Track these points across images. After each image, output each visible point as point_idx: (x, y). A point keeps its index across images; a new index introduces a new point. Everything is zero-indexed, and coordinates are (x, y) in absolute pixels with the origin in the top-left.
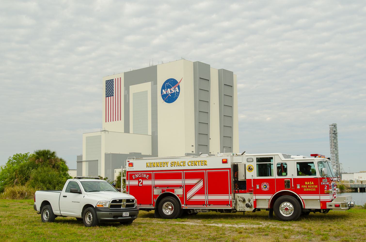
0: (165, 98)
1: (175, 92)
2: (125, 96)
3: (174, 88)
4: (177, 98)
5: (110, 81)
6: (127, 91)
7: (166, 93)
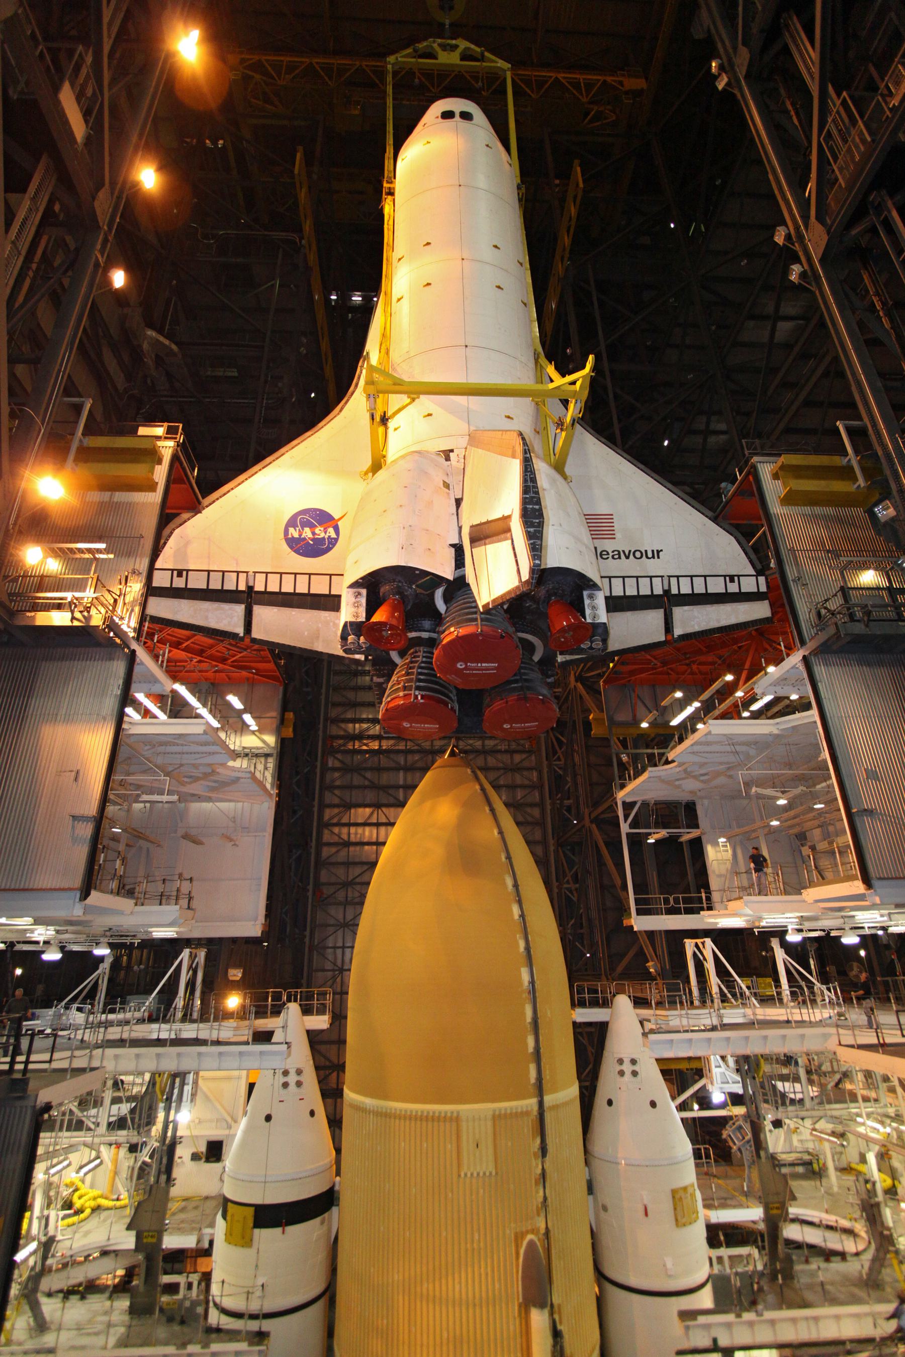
4: (329, 549)
7: (300, 535)
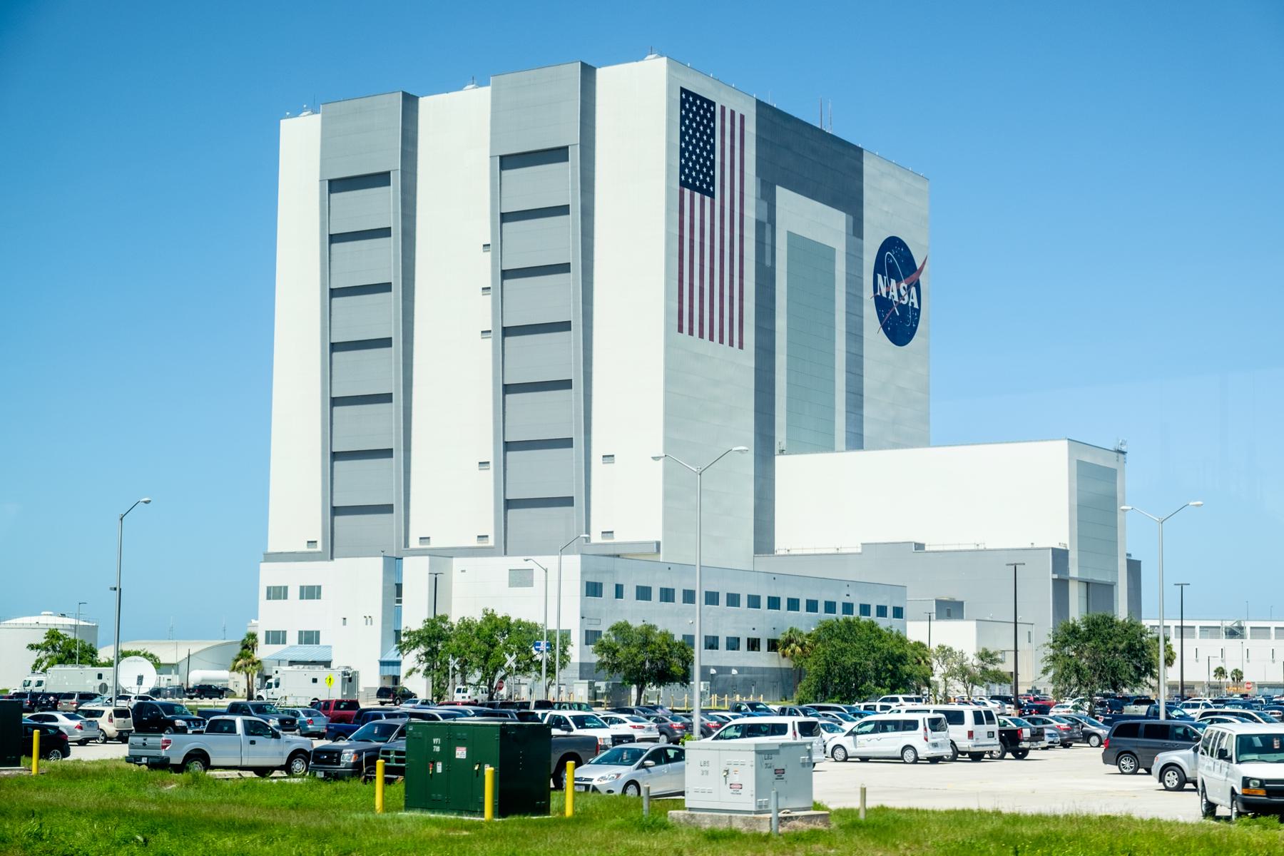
3: (909, 287)
6: (765, 205)
7: (888, 293)
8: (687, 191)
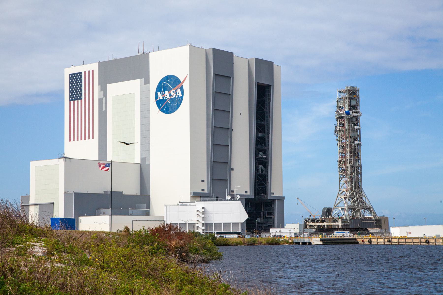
0: (162, 105)
1: (177, 96)
2: (100, 100)
4: (178, 106)
5: (77, 75)
6: (103, 92)
7: (163, 97)
8: (72, 102)
